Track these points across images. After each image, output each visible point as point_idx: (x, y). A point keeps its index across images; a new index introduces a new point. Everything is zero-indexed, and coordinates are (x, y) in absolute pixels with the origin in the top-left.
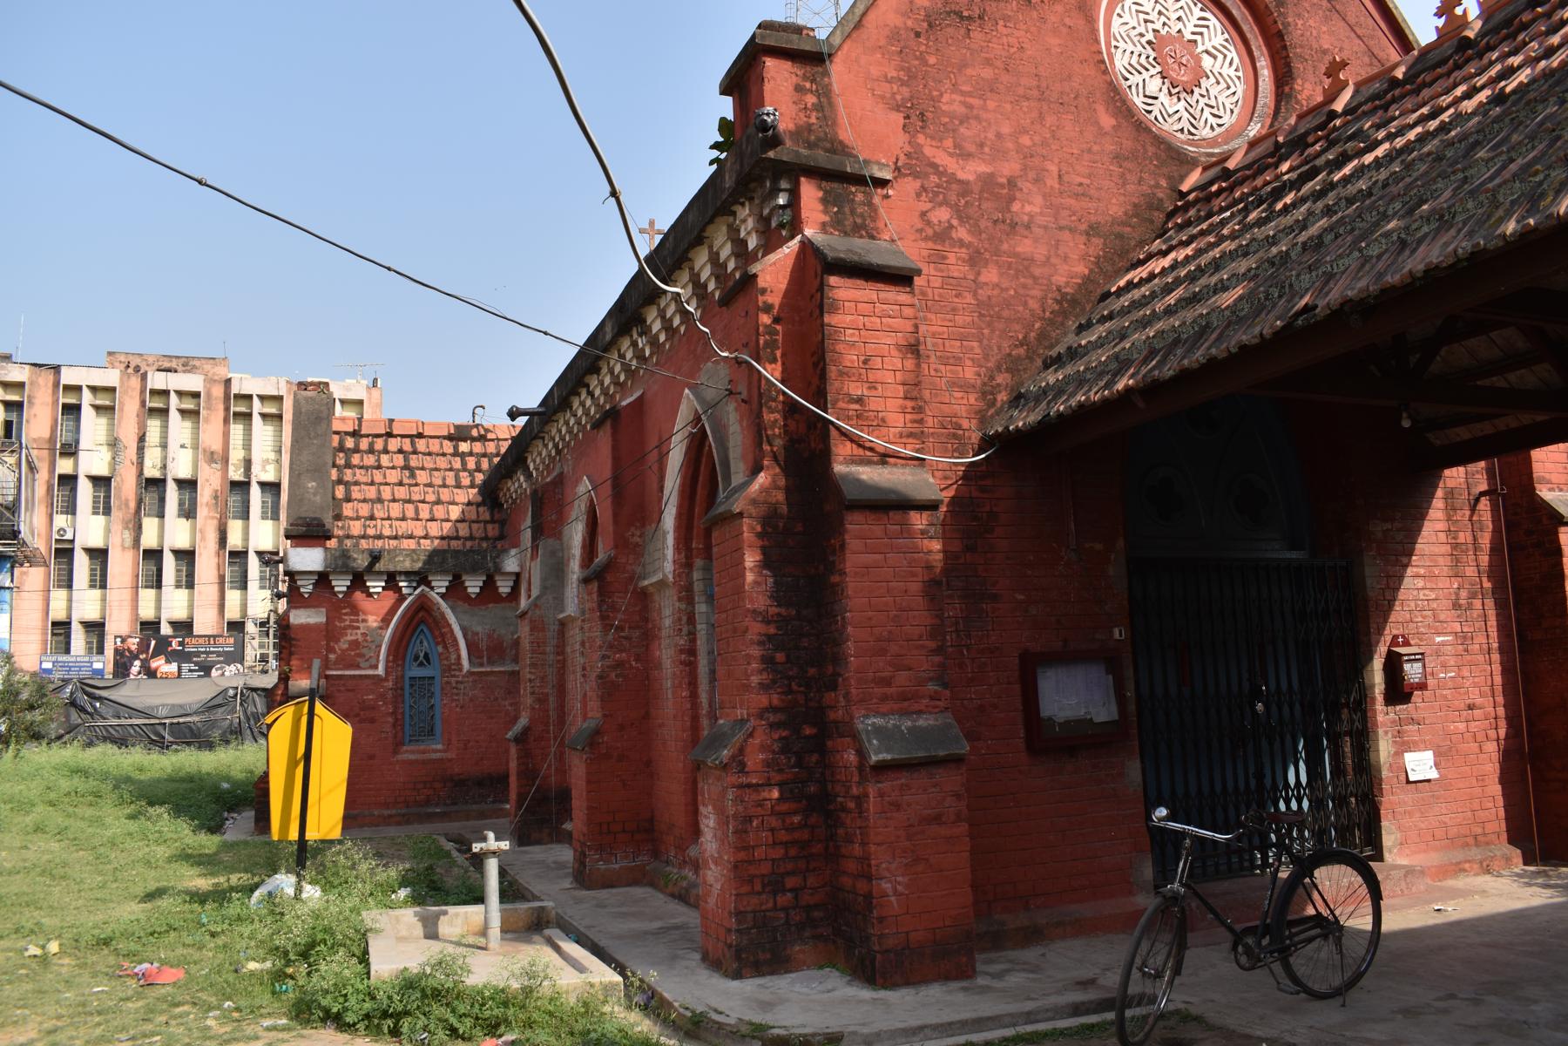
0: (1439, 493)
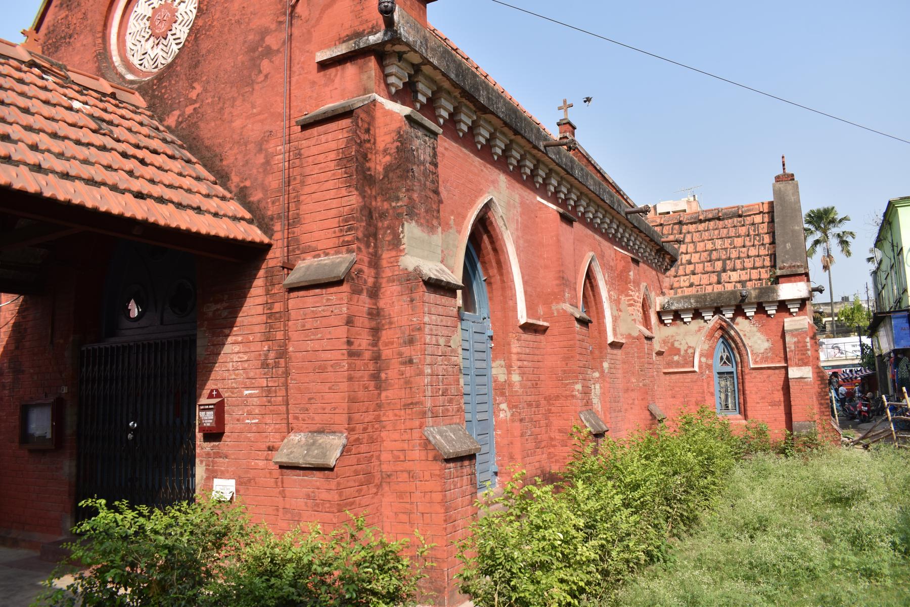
0: (261, 273)
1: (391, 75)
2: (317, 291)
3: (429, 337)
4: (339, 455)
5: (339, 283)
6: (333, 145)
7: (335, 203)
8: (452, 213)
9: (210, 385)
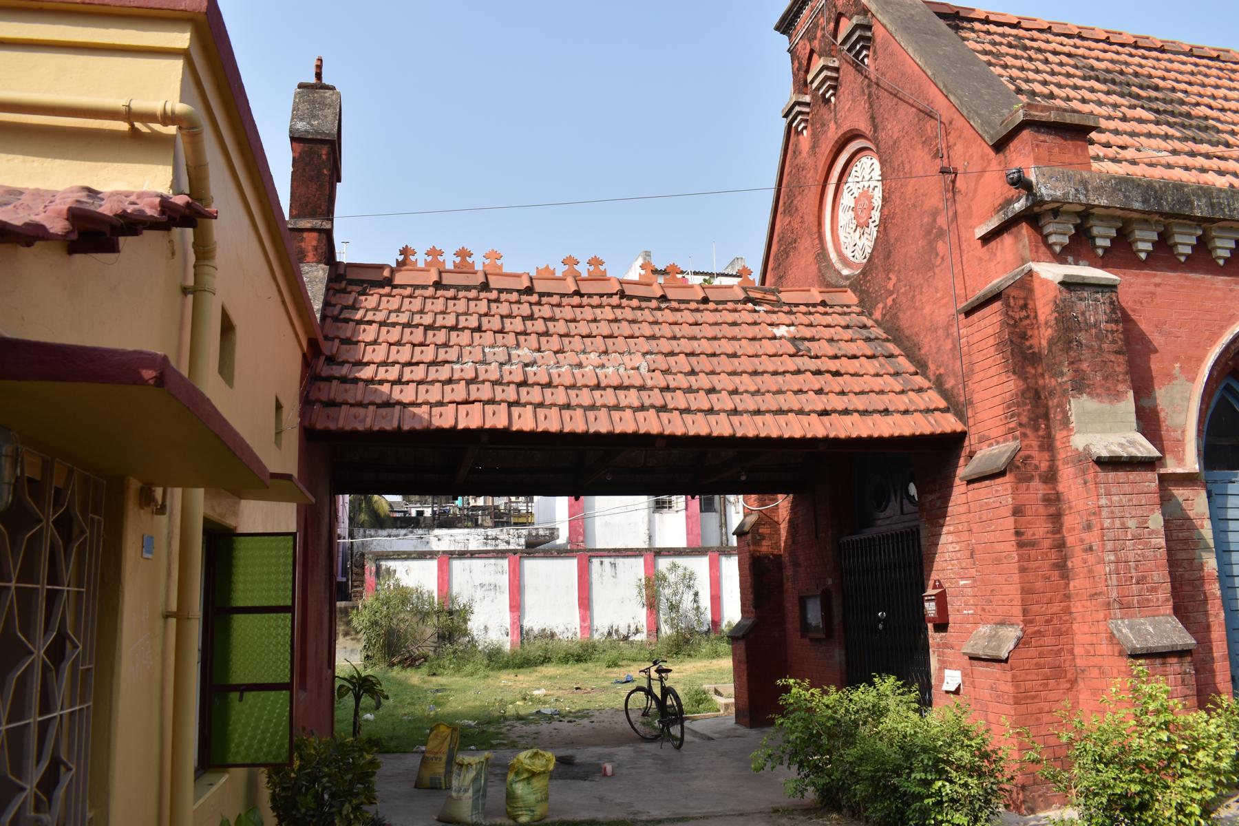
1: (1050, 234)
2: (987, 482)
3: (1109, 521)
4: (1012, 647)
5: (1001, 474)
6: (990, 330)
7: (998, 390)
8: (1177, 359)
9: (934, 576)
